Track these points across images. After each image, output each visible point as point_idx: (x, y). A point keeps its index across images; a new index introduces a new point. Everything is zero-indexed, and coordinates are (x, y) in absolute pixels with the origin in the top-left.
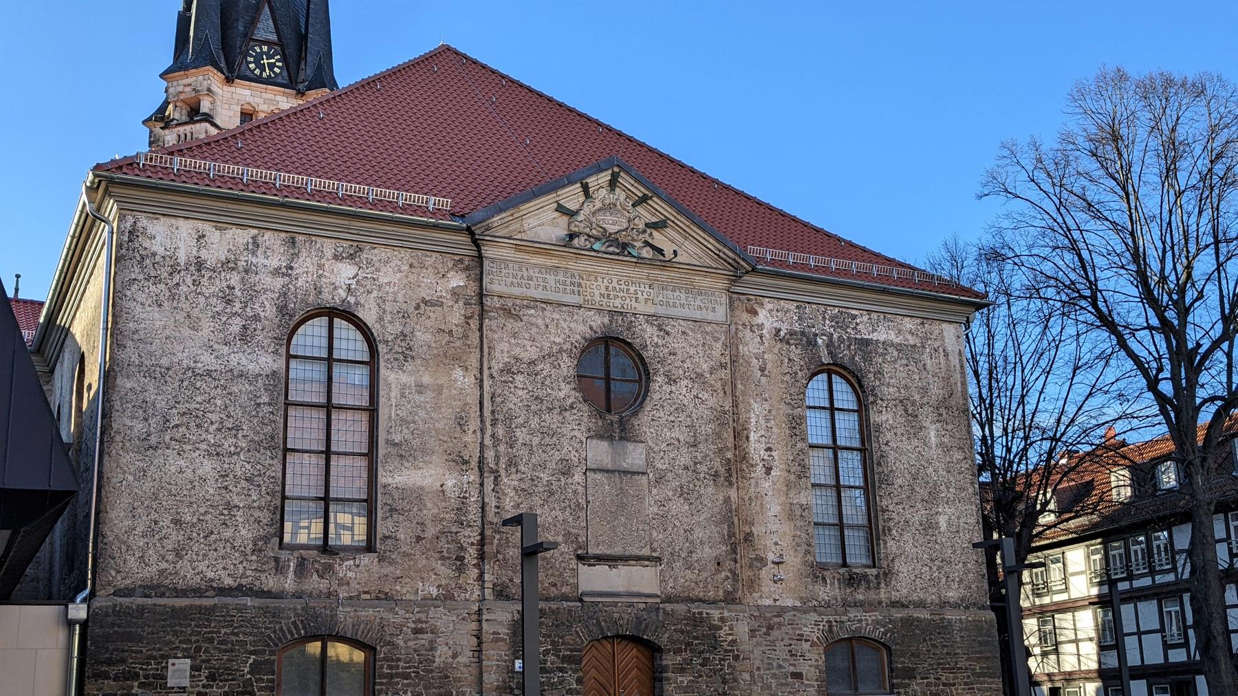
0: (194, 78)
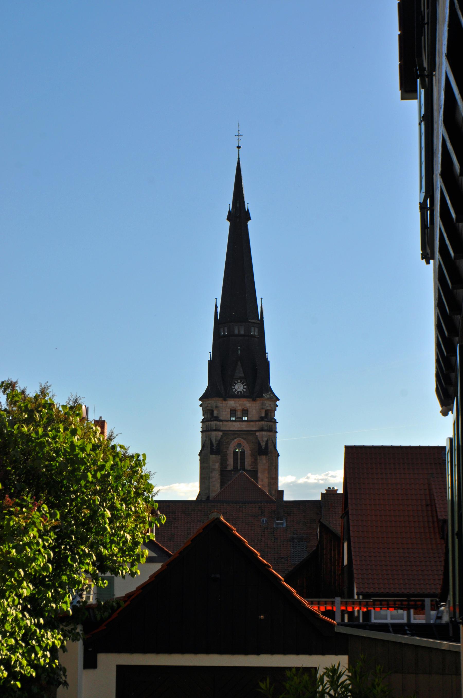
0: (211, 401)
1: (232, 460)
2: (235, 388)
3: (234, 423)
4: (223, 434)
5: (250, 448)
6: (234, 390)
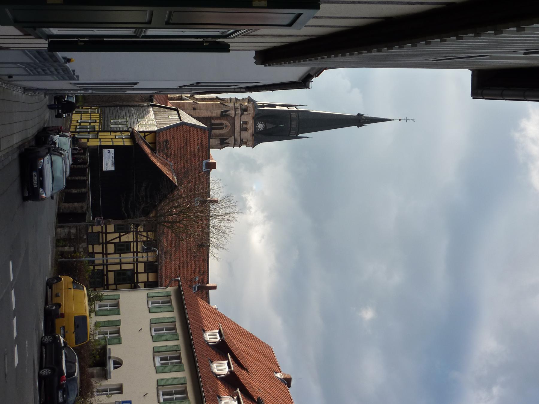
1: (218, 122)
3: (239, 123)
4: (233, 117)
5: (225, 133)
6: (259, 123)
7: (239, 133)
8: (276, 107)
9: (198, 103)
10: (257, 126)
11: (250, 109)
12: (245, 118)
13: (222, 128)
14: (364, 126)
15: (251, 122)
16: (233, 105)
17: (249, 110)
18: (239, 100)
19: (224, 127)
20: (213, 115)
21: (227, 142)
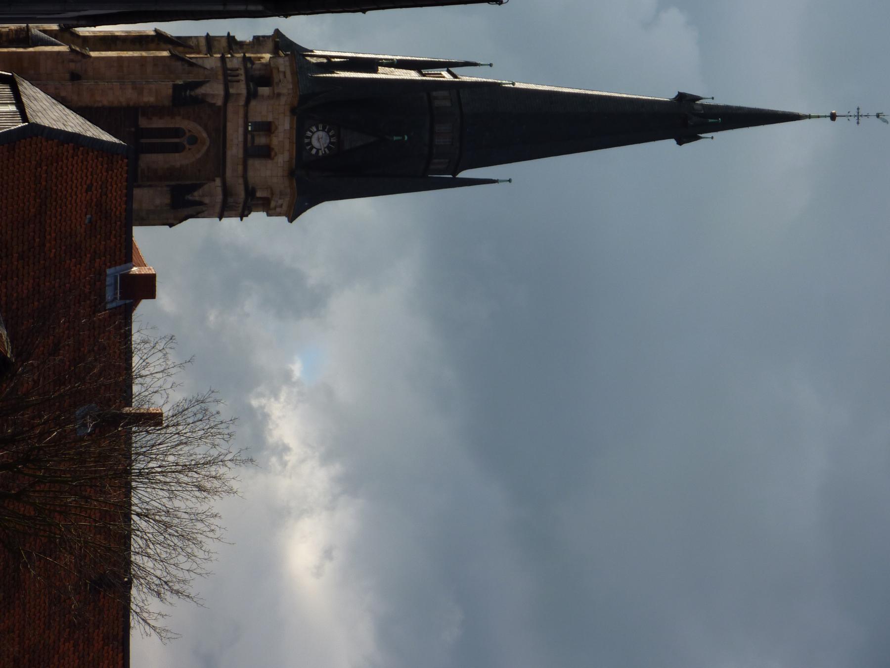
2: (318, 130)
3: (241, 130)
6: (314, 129)
7: (240, 168)
8: (376, 71)
9: (90, 57)
10: (306, 141)
11: (281, 76)
12: (261, 111)
13: (177, 149)
14: (700, 138)
15: (285, 125)
16: (219, 64)
17: (276, 80)
18: (241, 44)
19: (185, 143)
20: (146, 99)
21: (197, 199)
